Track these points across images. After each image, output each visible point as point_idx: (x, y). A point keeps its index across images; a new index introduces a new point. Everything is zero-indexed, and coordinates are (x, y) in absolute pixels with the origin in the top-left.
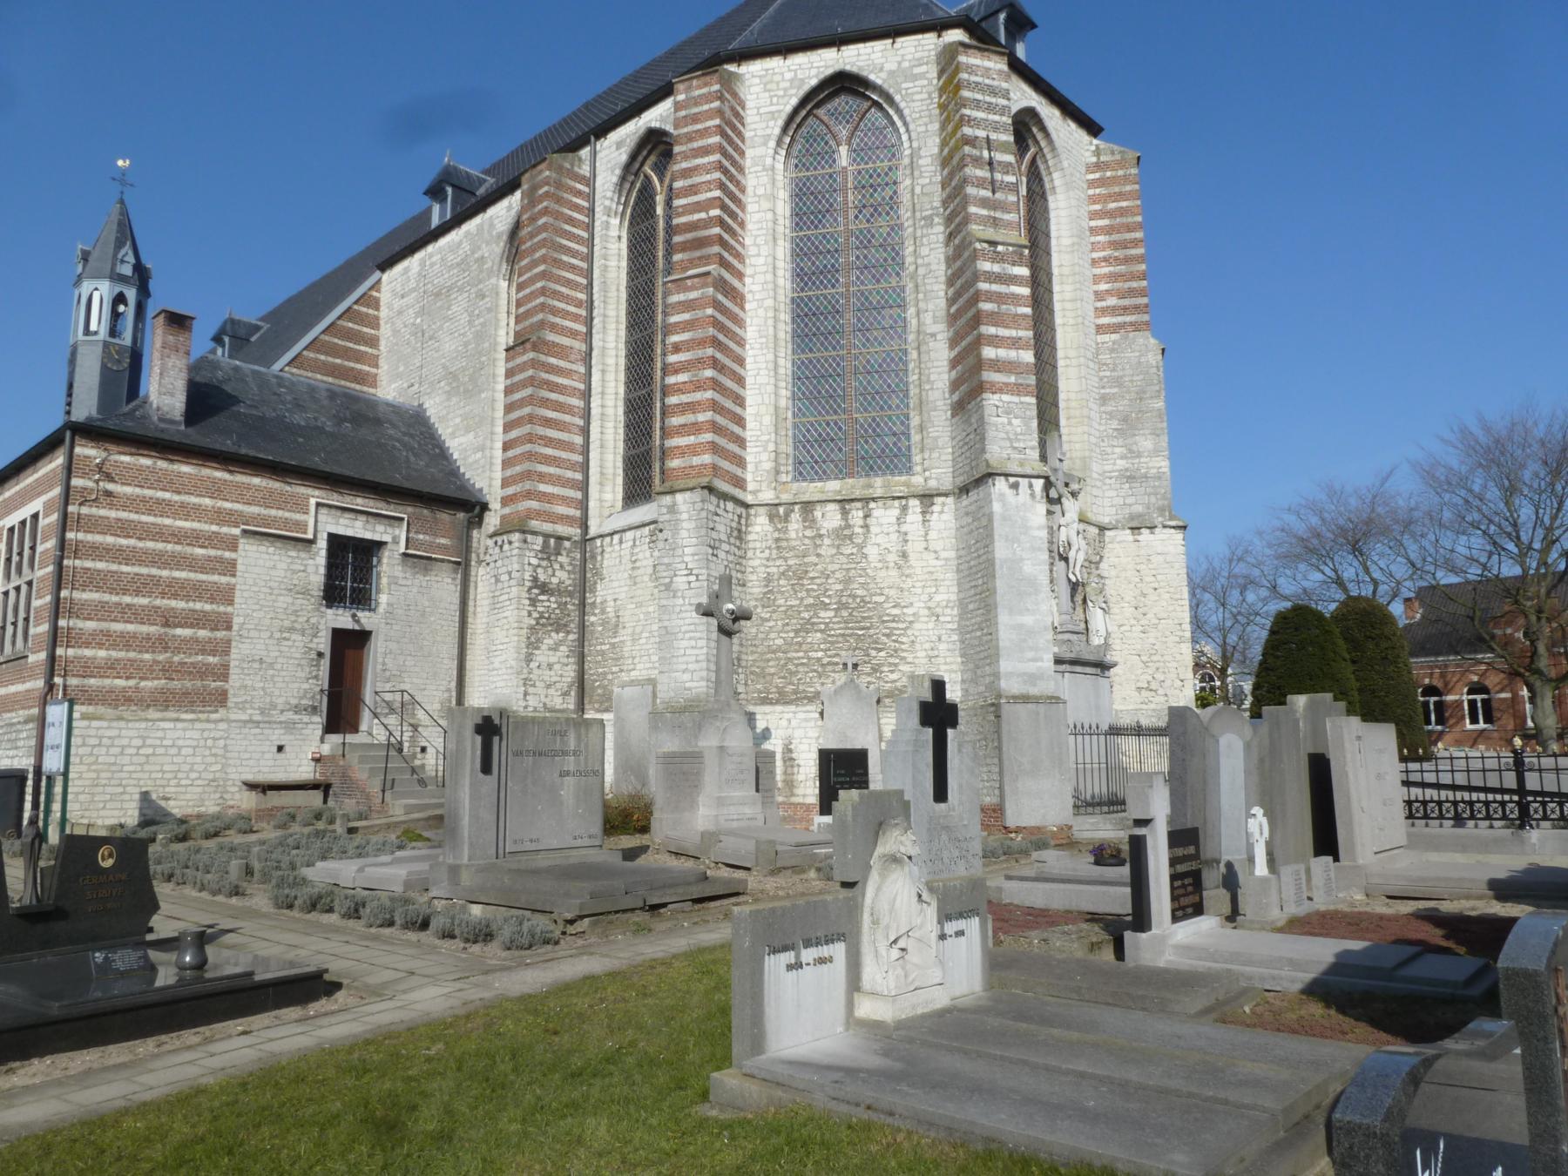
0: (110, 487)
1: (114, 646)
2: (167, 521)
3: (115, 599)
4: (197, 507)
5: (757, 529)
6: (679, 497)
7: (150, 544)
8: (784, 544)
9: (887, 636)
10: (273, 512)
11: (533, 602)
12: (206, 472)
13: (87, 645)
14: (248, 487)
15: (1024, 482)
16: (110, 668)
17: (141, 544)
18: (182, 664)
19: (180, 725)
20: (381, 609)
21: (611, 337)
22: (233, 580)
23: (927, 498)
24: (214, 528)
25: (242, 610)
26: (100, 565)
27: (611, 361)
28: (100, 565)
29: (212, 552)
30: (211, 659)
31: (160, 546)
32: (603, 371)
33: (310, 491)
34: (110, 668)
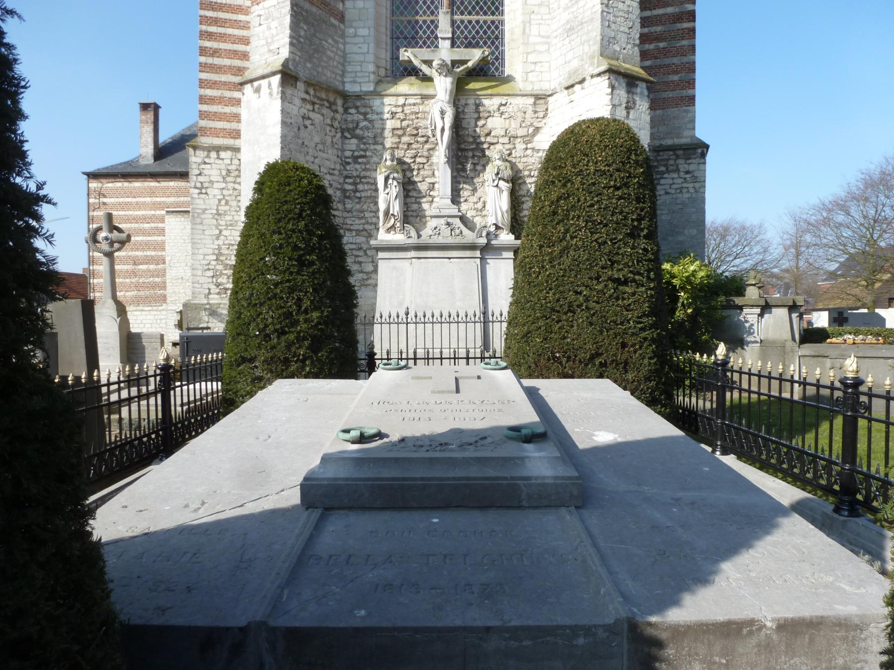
0: (105, 200)
2: (131, 213)
4: (144, 203)
10: (182, 199)
12: (146, 184)
14: (168, 188)
15: (264, 83)
19: (143, 313)
22: (164, 238)
24: (153, 212)
25: (169, 253)
29: (153, 225)
30: (157, 279)
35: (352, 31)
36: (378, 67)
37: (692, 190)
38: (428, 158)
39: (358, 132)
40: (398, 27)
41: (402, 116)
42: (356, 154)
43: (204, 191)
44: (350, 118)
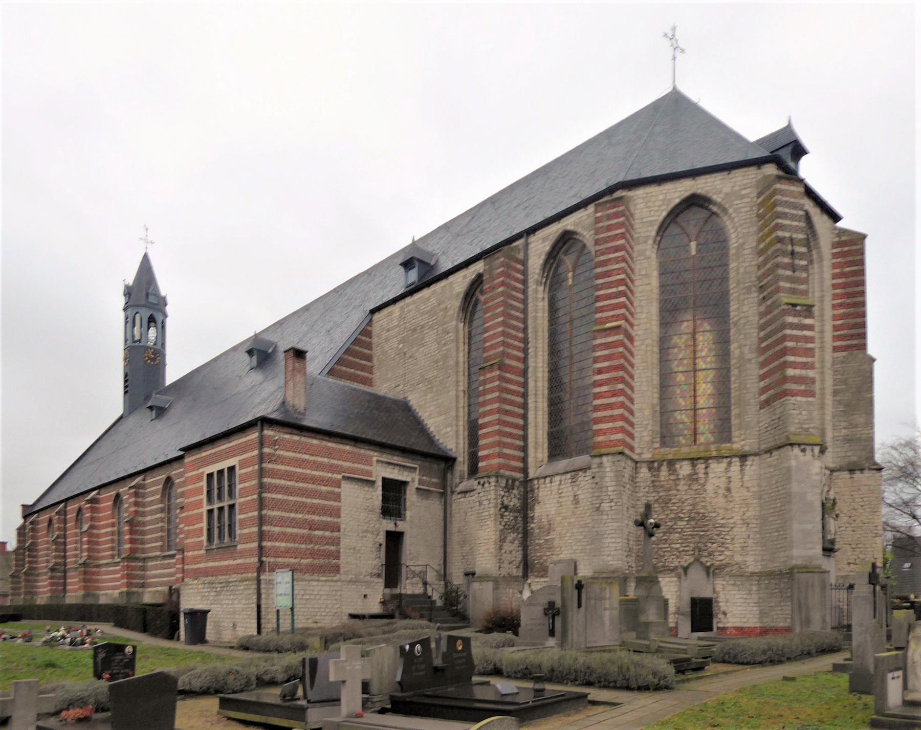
2: (308, 471)
3: (287, 515)
4: (321, 464)
5: (642, 475)
6: (605, 459)
7: (301, 485)
8: (657, 484)
9: (718, 535)
10: (356, 465)
11: (502, 516)
12: (324, 443)
14: (344, 451)
18: (319, 550)
20: (408, 518)
21: (540, 360)
23: (743, 457)
24: (330, 475)
25: (345, 520)
26: (280, 496)
27: (540, 375)
28: (280, 496)
29: (330, 489)
31: (305, 485)
32: (536, 381)
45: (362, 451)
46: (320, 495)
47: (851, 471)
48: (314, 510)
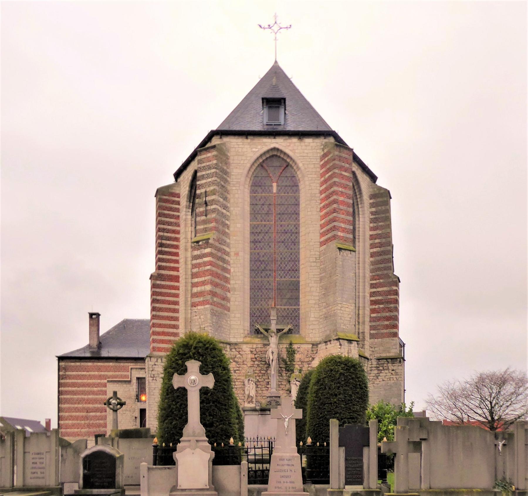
1: (73, 420)
3: (73, 406)
12: (95, 364)
13: (66, 420)
16: (73, 426)
17: (78, 389)
18: (93, 423)
24: (99, 381)
29: (99, 389)
33: (129, 364)
34: (73, 426)
35: (233, 315)
36: (244, 330)
37: (395, 379)
38: (266, 371)
39: (236, 359)
40: (253, 311)
41: (255, 353)
42: (235, 369)
43: (155, 379)
44: (232, 353)
45: (122, 364)
46: (93, 393)
47: (326, 342)
48: (88, 401)
